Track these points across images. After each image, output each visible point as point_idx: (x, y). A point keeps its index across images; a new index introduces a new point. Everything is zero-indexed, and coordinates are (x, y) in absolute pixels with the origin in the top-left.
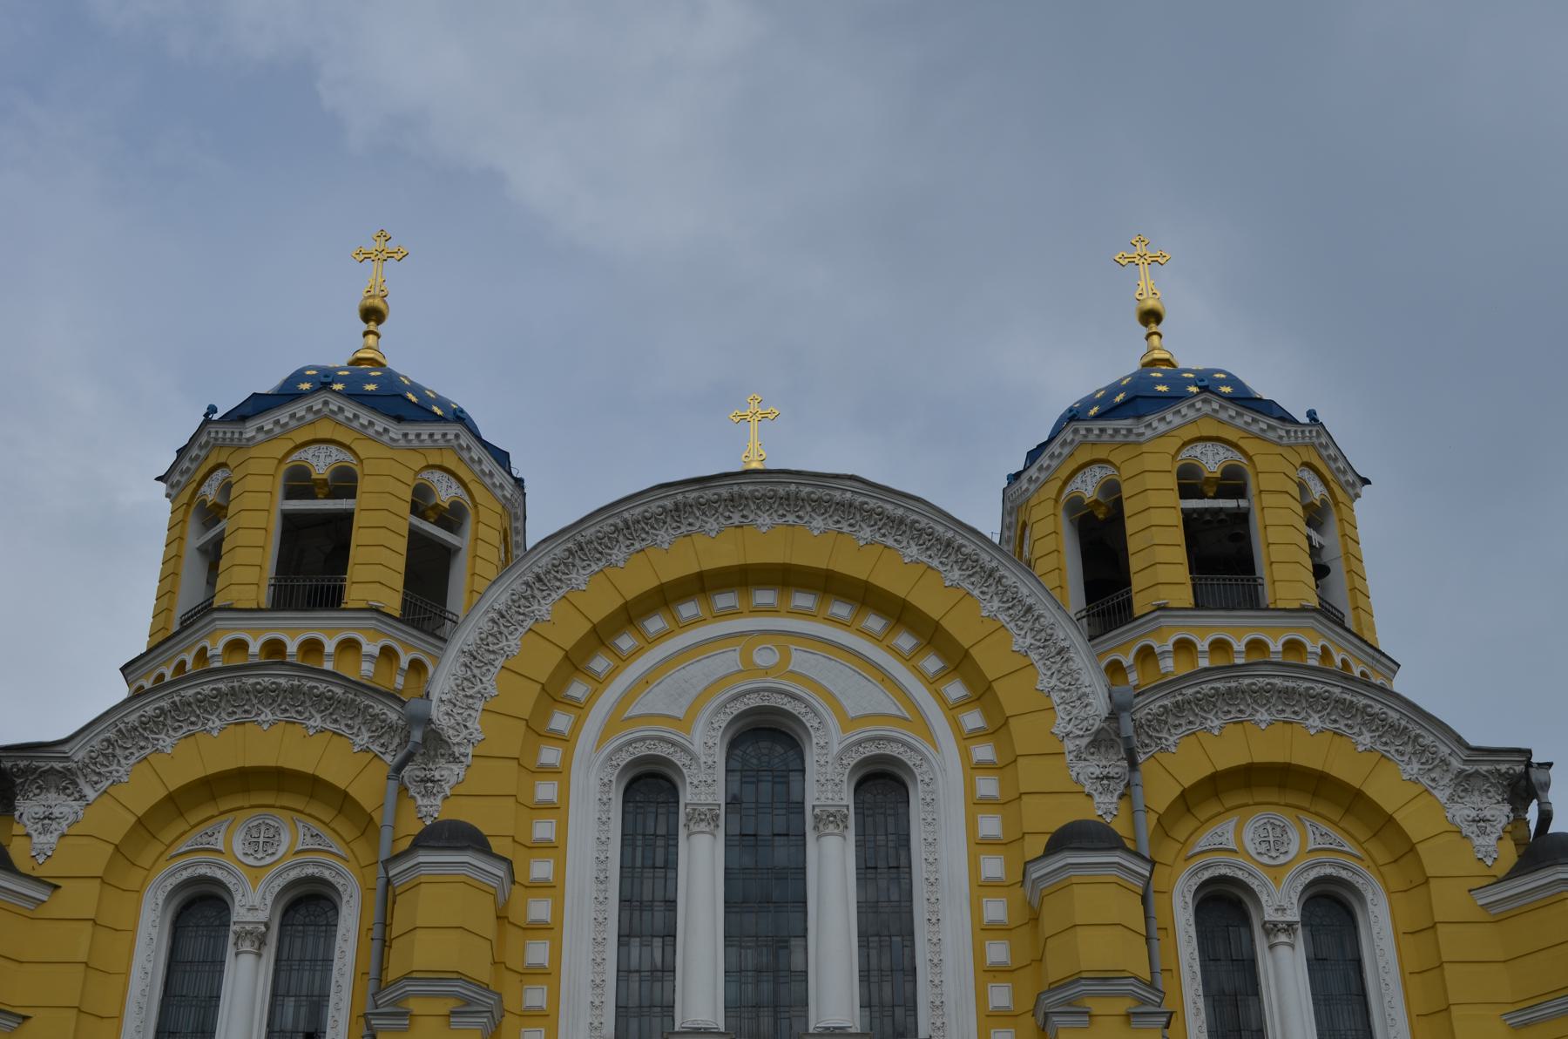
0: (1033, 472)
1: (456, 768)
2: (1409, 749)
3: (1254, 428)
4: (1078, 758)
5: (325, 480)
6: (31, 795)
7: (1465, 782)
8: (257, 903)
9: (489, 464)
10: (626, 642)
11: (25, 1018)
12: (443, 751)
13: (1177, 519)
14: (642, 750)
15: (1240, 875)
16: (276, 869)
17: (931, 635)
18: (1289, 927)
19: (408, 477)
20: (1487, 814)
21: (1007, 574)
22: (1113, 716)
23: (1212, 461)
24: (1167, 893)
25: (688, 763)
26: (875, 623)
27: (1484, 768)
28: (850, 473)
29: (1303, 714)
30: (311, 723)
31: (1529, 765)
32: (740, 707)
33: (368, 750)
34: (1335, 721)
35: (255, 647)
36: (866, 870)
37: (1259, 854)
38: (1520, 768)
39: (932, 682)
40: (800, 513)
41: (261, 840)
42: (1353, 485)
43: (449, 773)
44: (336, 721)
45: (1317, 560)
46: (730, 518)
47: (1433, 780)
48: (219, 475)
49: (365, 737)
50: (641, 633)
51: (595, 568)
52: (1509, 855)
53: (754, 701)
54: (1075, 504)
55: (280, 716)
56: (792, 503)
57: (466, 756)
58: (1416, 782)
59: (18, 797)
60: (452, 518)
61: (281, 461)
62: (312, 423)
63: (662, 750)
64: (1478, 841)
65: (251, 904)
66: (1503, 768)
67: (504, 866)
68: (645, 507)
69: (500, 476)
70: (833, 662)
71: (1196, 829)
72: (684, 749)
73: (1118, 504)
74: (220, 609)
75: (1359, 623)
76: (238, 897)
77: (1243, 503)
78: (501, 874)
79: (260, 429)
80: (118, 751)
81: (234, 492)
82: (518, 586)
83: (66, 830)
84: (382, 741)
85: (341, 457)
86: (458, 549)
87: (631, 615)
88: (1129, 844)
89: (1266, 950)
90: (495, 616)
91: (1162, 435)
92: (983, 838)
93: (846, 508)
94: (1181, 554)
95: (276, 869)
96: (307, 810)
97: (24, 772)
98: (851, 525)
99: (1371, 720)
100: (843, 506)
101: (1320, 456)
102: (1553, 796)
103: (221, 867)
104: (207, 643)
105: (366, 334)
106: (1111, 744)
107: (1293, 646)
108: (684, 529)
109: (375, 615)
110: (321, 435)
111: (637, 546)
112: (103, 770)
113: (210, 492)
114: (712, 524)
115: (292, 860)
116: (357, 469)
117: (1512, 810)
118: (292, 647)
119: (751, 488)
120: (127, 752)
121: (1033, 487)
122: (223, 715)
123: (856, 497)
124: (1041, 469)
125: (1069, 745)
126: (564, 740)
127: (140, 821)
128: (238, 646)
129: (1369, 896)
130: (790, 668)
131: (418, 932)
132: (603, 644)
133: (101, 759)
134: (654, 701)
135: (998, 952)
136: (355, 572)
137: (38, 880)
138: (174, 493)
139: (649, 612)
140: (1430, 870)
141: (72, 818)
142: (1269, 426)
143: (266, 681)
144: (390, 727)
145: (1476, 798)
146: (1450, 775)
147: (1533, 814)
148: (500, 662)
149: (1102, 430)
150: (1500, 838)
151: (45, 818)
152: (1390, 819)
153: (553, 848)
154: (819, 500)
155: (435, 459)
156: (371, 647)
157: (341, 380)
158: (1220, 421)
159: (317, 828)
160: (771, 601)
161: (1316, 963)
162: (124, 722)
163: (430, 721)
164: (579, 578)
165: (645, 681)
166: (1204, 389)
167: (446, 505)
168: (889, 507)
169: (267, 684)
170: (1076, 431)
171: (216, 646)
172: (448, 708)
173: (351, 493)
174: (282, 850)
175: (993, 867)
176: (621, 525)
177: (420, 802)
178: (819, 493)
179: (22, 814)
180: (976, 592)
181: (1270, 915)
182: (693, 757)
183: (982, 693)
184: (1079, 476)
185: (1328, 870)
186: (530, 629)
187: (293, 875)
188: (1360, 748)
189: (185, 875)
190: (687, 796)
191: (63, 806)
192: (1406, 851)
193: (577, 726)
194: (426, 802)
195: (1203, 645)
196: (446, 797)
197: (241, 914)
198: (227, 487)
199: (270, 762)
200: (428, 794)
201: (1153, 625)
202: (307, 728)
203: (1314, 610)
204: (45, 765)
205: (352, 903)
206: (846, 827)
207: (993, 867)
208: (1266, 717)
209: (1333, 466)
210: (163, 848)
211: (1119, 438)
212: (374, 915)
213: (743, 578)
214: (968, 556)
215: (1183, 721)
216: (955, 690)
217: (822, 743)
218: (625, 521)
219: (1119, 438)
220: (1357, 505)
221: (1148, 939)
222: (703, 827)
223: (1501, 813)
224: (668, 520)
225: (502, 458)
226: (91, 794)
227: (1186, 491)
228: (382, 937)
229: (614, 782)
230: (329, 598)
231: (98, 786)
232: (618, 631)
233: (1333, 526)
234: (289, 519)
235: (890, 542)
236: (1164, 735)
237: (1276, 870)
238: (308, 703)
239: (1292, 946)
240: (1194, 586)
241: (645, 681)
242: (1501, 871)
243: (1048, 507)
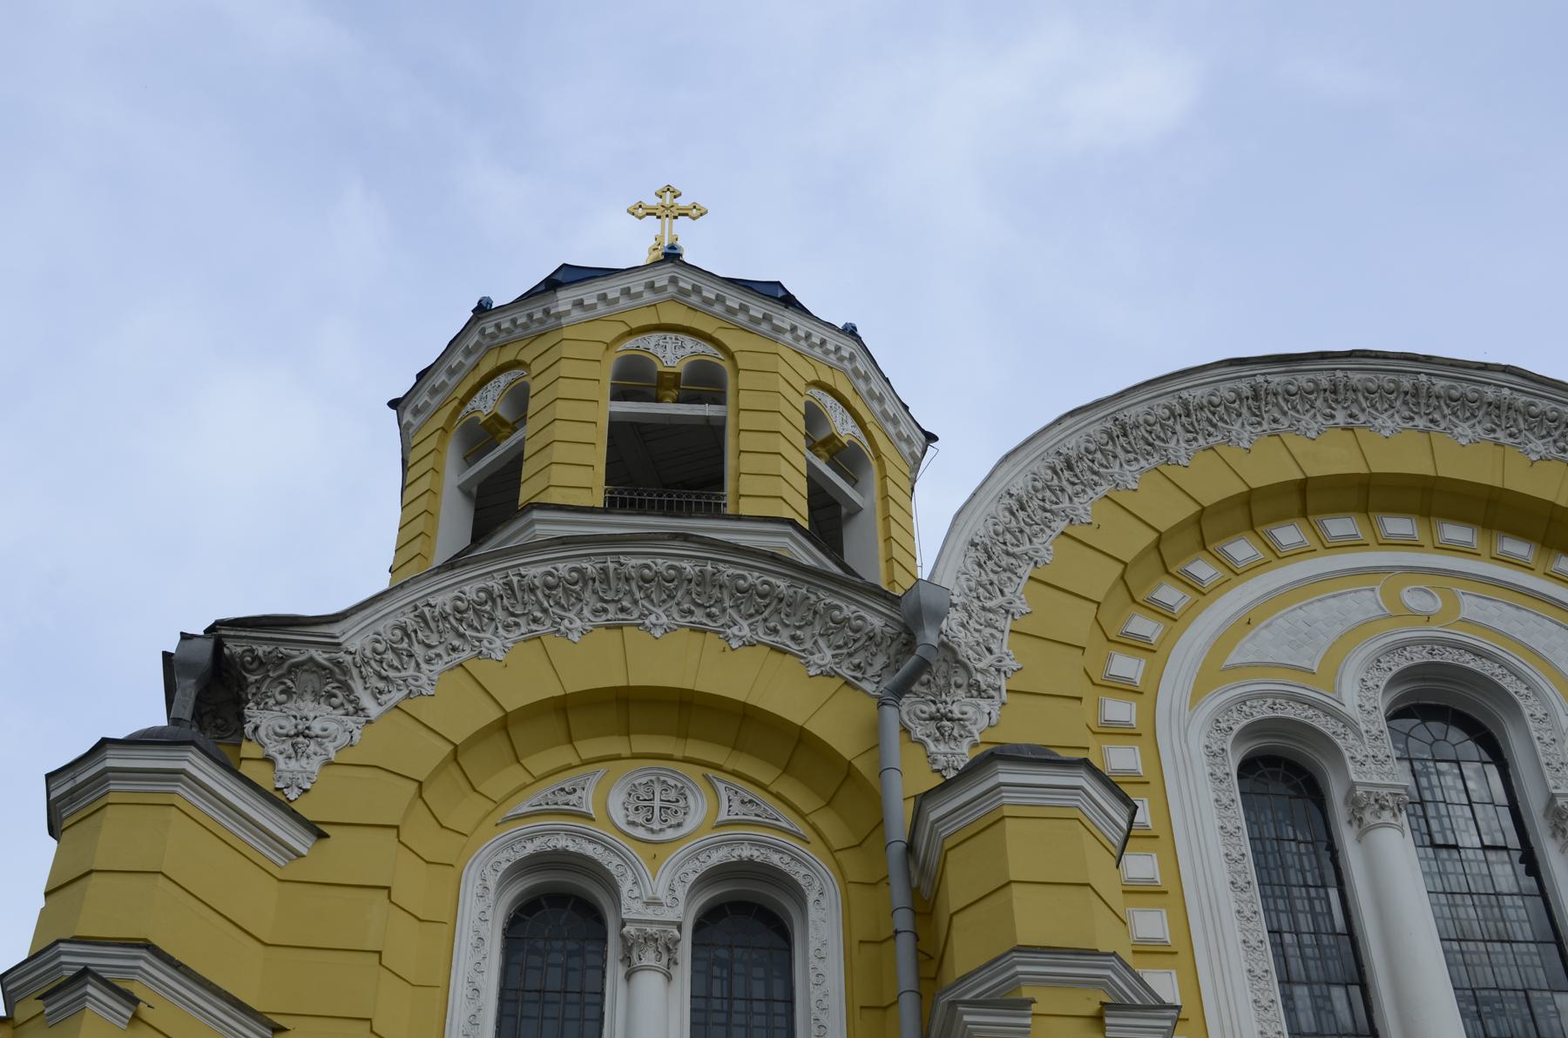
1: (982, 702)
5: (678, 375)
6: (271, 702)
8: (662, 893)
12: (960, 681)
25: (1340, 730)
28: (1504, 363)
33: (831, 674)
40: (1437, 416)
41: (657, 804)
44: (775, 631)
46: (1333, 417)
49: (825, 657)
56: (1423, 401)
59: (251, 705)
65: (650, 894)
67: (1125, 813)
68: (1212, 387)
70: (1524, 612)
80: (418, 650)
83: (333, 755)
84: (856, 661)
97: (261, 663)
98: (1511, 435)
100: (1498, 408)
103: (592, 839)
108: (1265, 426)
109: (790, 529)
112: (392, 674)
113: (488, 403)
116: (726, 365)
120: (432, 653)
122: (586, 613)
123: (1516, 394)
130: (1464, 614)
131: (1013, 886)
133: (389, 656)
141: (343, 739)
143: (661, 564)
144: (870, 638)
151: (297, 735)
154: (1462, 399)
155: (827, 378)
162: (429, 605)
165: (1246, 622)
167: (845, 440)
169: (662, 569)
173: (718, 398)
174: (691, 823)
176: (1178, 410)
177: (932, 747)
179: (256, 728)
182: (1348, 723)
186: (1063, 533)
187: (717, 857)
189: (531, 848)
194: (942, 748)
200: (942, 736)
205: (824, 903)
218: (1185, 404)
224: (1244, 411)
226: (373, 709)
229: (1229, 751)
231: (383, 698)
234: (619, 430)
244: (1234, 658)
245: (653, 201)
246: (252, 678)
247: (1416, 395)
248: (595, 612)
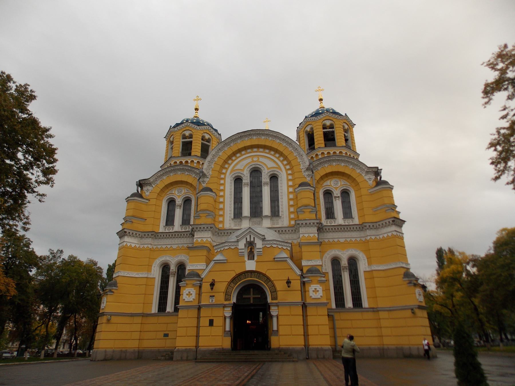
0: (300, 127)
1: (208, 179)
2: (358, 168)
3: (335, 117)
4: (304, 172)
7: (367, 173)
9: (214, 132)
10: (234, 158)
11: (146, 219)
13: (322, 133)
14: (236, 175)
15: (330, 189)
16: (182, 195)
17: (281, 154)
18: (338, 197)
19: (200, 134)
20: (371, 178)
21: (293, 143)
22: (309, 165)
23: (328, 123)
24: (318, 192)
26: (272, 153)
27: (370, 170)
29: (341, 163)
30: (186, 173)
31: (378, 169)
32: (251, 167)
34: (346, 164)
35: (178, 162)
36: (271, 191)
37: (334, 186)
38: (376, 170)
39: (282, 162)
42: (353, 125)
43: (207, 180)
45: (347, 138)
47: (362, 173)
48: (172, 136)
50: (236, 157)
51: (228, 147)
52: (375, 184)
53: (254, 166)
54: (306, 132)
55: (181, 173)
57: (209, 177)
58: (359, 173)
60: (209, 141)
61: (181, 133)
62: (185, 127)
63: (239, 174)
64: (369, 182)
66: (374, 170)
67: (215, 193)
69: (216, 134)
71: (324, 182)
72: (243, 174)
73: (313, 131)
74: (173, 157)
75: (353, 148)
76: (177, 200)
77: (333, 130)
78: (214, 195)
79: (178, 129)
80: (157, 179)
81: (174, 139)
82: (216, 151)
85: (190, 132)
86: (210, 145)
87: (234, 154)
88: (312, 185)
89: (335, 202)
90: (213, 155)
91: (320, 119)
92: (290, 185)
93: (267, 135)
94: (322, 138)
95: (182, 195)
96: (186, 187)
97: (144, 183)
99: (352, 163)
101: (347, 121)
102: (382, 174)
103: (174, 196)
104: (171, 162)
105: (196, 113)
106: (309, 170)
107: (341, 152)
109: (196, 156)
110: (187, 129)
111: (235, 143)
114: (246, 139)
115: (183, 195)
117: (375, 177)
118: (184, 162)
119: (252, 132)
121: (300, 129)
124: (301, 126)
125: (303, 170)
126: (225, 174)
127: (161, 190)
128: (176, 162)
129: (351, 191)
132: (230, 159)
134: (238, 167)
135: (292, 203)
136: (193, 150)
137: (146, 199)
138: (167, 140)
139: (237, 153)
140: (361, 187)
141: (151, 190)
142: (338, 117)
145: (369, 175)
146: (365, 172)
147: (379, 178)
148: (214, 162)
149: (310, 119)
150: (373, 181)
152: (355, 179)
153: (223, 190)
156: (196, 161)
157: (190, 120)
158: (329, 116)
159: (188, 189)
160: (256, 150)
161: (343, 202)
163: (203, 172)
164: (226, 149)
165: (237, 164)
166: (327, 111)
168: (274, 134)
170: (306, 120)
171: (172, 163)
172: (206, 170)
173: (192, 138)
175: (291, 190)
178: (263, 132)
180: (288, 147)
181: (335, 195)
182: (244, 175)
183: (289, 163)
184: (307, 127)
185: (345, 188)
187: (184, 196)
188: (350, 168)
189: (169, 197)
190: (244, 181)
191: (150, 188)
192: (358, 184)
193: (227, 171)
195: (326, 153)
196: (206, 184)
197: (177, 203)
198: (173, 138)
199: (180, 180)
200: (204, 183)
201: (318, 150)
202: (185, 174)
203: (344, 146)
204: (147, 182)
206: (268, 185)
207: (291, 190)
208: (335, 164)
209: (349, 122)
210: (165, 193)
211: (313, 120)
212: (196, 201)
213: (252, 147)
214: (287, 141)
215: (321, 165)
216: (285, 162)
217: (264, 172)
218: (233, 139)
219: (313, 120)
220: (353, 129)
221: (314, 200)
222: (246, 186)
223: (373, 177)
225: (216, 131)
226: (154, 186)
227: (324, 128)
228: (197, 205)
230: (190, 154)
232: (232, 157)
233: (349, 132)
234: (183, 142)
235: (275, 140)
236: (318, 168)
237: (336, 188)
238: (185, 170)
239: (339, 200)
240: (325, 144)
241: (237, 164)
242: (373, 187)
243: (302, 133)
244: (234, 169)
245: (196, 98)
246: (143, 185)
247: (258, 134)
248: (174, 173)
